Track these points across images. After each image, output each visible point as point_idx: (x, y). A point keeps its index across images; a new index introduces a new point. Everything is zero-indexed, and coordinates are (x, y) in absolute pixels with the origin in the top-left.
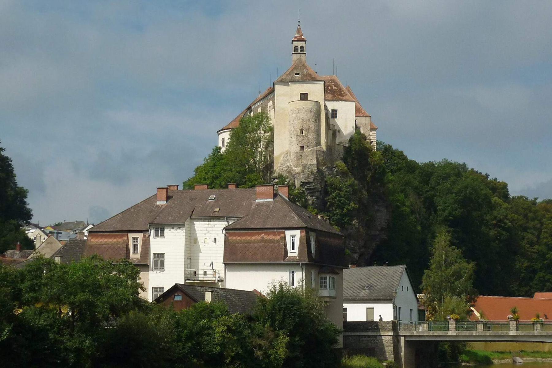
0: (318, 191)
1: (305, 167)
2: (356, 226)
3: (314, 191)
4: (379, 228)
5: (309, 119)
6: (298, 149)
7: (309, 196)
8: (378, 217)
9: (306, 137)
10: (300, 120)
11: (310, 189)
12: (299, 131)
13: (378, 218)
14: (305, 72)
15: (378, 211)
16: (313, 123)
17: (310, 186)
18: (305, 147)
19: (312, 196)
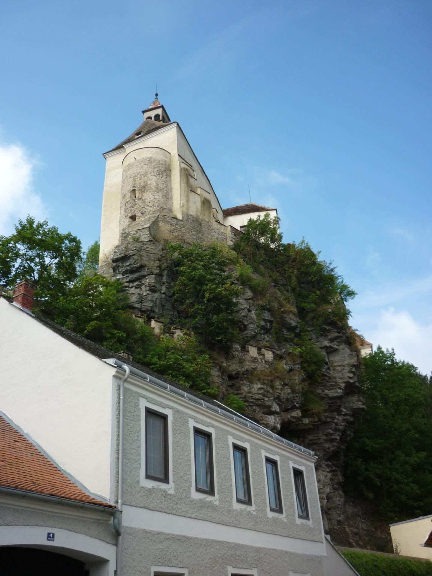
1: (126, 237)
2: (266, 356)
3: (142, 273)
5: (145, 173)
7: (132, 287)
8: (336, 364)
9: (140, 199)
10: (131, 179)
11: (132, 272)
12: (128, 195)
13: (336, 366)
15: (330, 351)
16: (154, 177)
17: (130, 264)
18: (138, 215)
19: (139, 287)
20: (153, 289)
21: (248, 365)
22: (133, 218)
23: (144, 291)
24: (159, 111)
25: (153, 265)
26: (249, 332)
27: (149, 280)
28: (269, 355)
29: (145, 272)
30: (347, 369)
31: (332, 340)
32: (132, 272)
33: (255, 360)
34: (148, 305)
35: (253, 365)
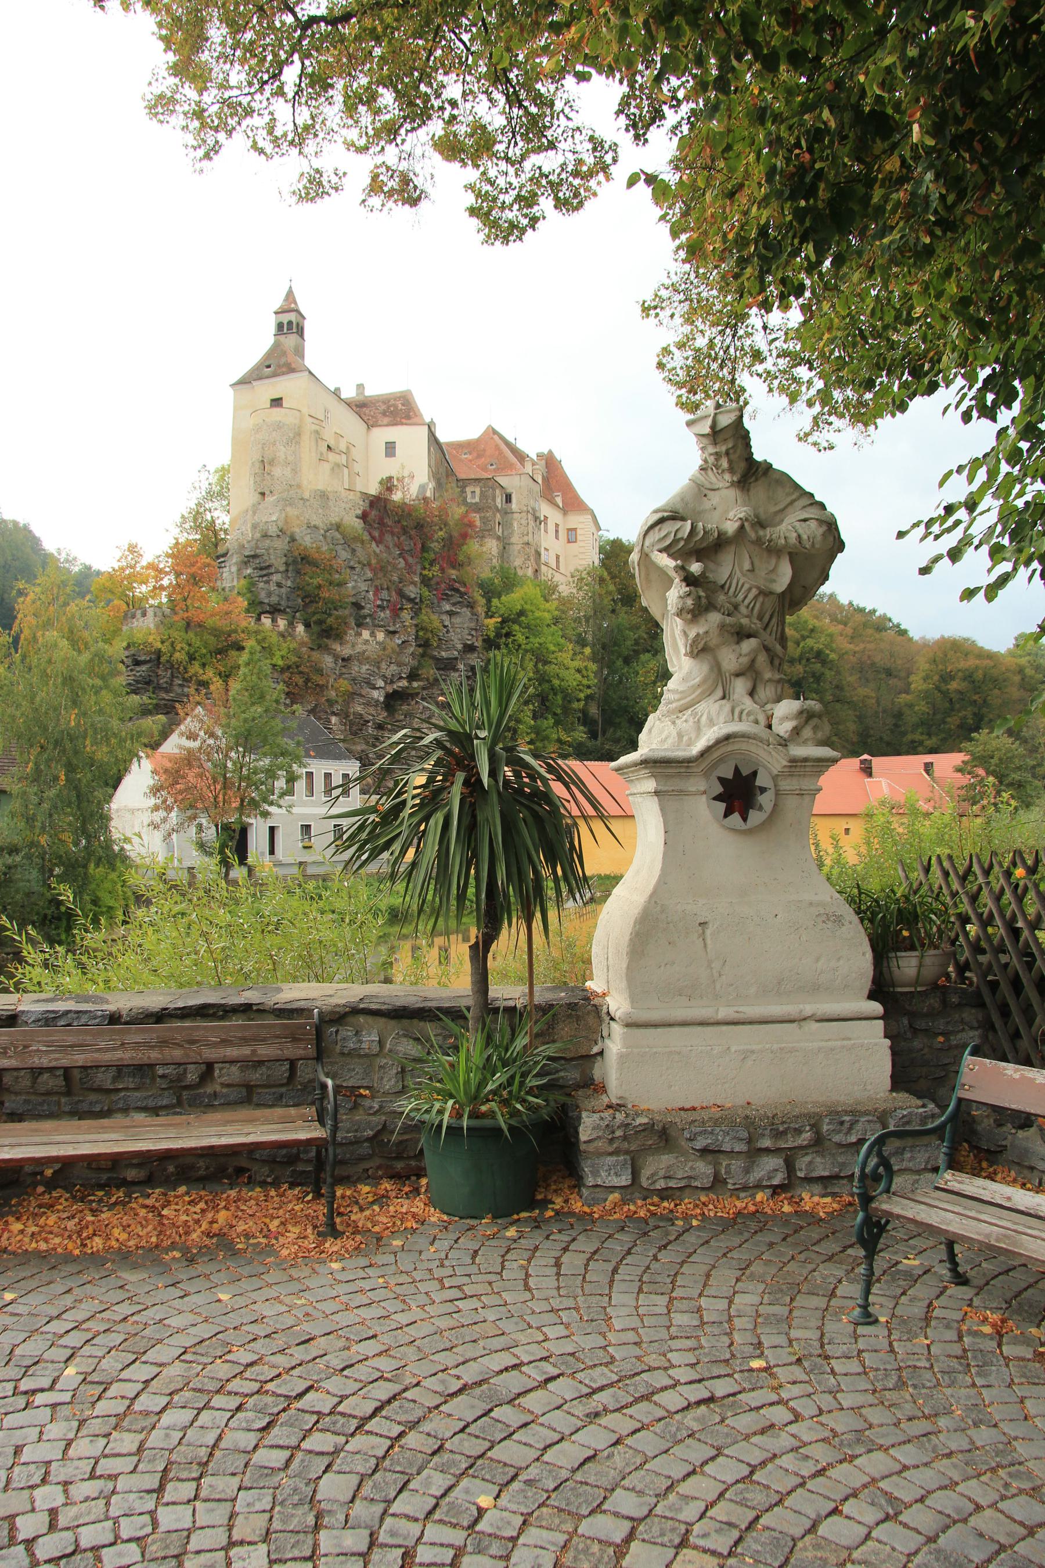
0: (277, 572)
4: (460, 647)
6: (257, 497)
11: (261, 569)
12: (257, 465)
14: (283, 360)
19: (267, 582)
20: (279, 585)
21: (360, 648)
22: (263, 494)
23: (273, 587)
24: (292, 317)
25: (279, 563)
26: (366, 611)
27: (276, 578)
28: (381, 636)
29: (272, 570)
30: (466, 631)
31: (454, 604)
32: (261, 569)
33: (366, 642)
34: (274, 599)
35: (364, 647)
